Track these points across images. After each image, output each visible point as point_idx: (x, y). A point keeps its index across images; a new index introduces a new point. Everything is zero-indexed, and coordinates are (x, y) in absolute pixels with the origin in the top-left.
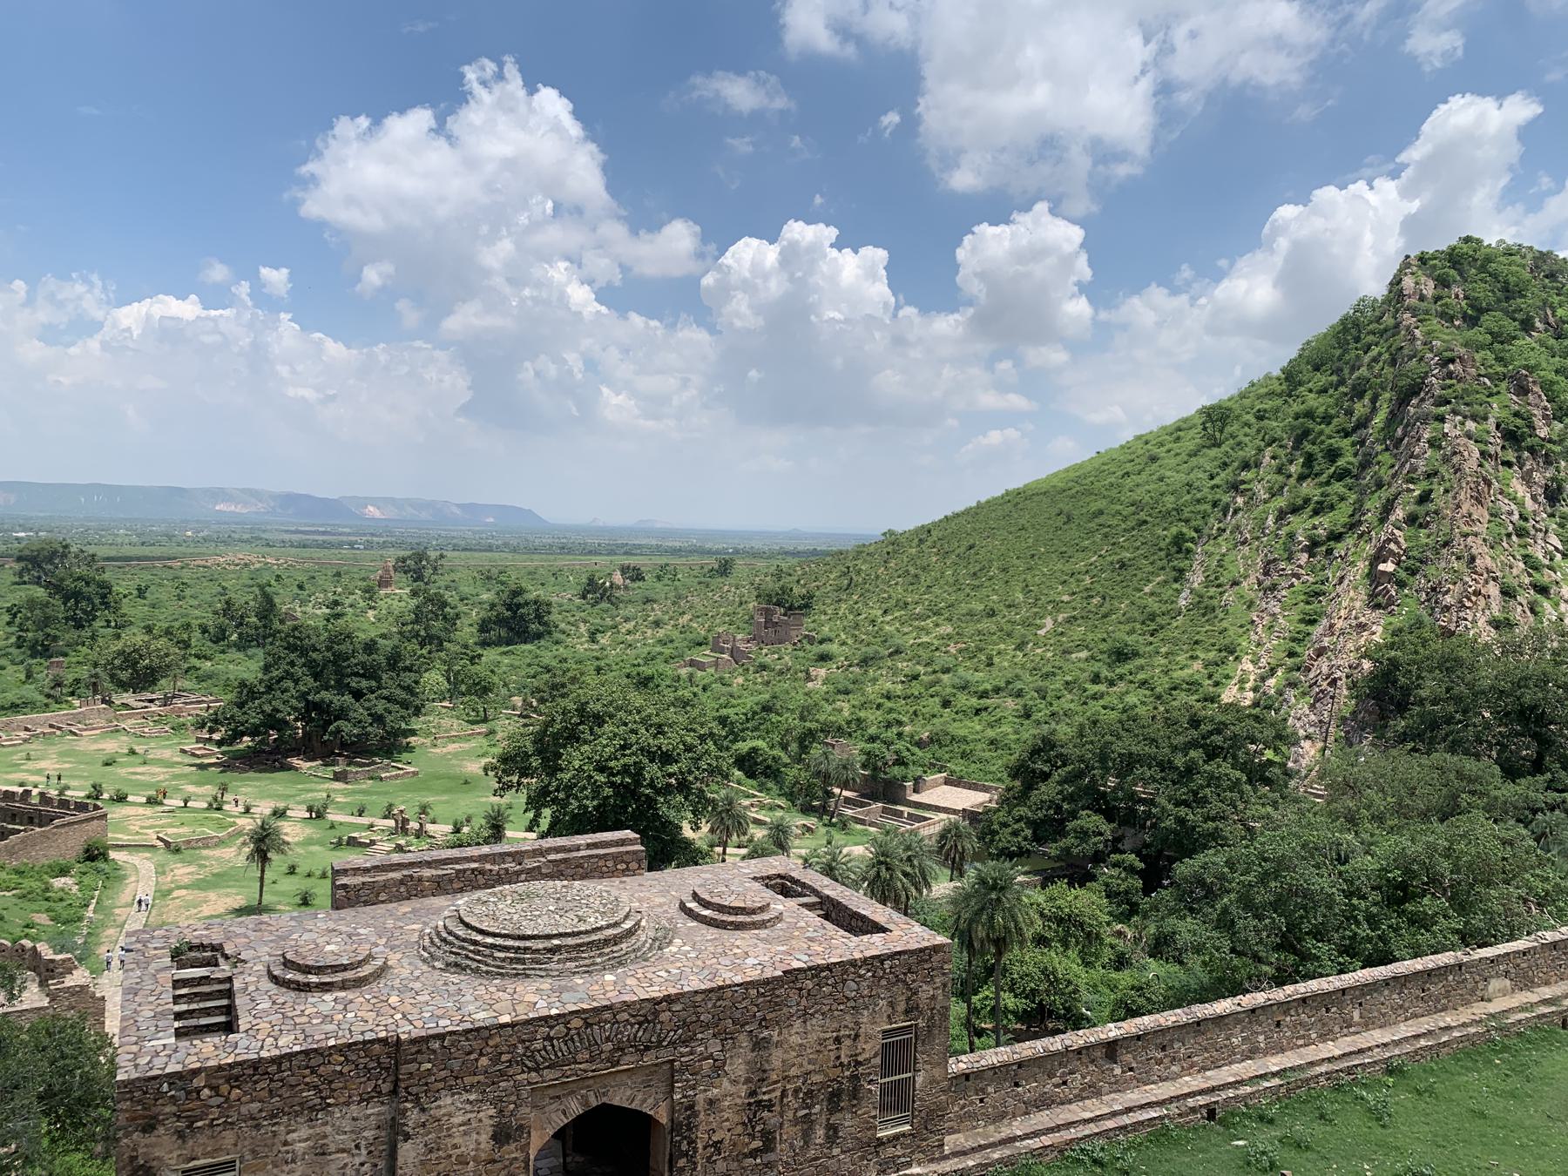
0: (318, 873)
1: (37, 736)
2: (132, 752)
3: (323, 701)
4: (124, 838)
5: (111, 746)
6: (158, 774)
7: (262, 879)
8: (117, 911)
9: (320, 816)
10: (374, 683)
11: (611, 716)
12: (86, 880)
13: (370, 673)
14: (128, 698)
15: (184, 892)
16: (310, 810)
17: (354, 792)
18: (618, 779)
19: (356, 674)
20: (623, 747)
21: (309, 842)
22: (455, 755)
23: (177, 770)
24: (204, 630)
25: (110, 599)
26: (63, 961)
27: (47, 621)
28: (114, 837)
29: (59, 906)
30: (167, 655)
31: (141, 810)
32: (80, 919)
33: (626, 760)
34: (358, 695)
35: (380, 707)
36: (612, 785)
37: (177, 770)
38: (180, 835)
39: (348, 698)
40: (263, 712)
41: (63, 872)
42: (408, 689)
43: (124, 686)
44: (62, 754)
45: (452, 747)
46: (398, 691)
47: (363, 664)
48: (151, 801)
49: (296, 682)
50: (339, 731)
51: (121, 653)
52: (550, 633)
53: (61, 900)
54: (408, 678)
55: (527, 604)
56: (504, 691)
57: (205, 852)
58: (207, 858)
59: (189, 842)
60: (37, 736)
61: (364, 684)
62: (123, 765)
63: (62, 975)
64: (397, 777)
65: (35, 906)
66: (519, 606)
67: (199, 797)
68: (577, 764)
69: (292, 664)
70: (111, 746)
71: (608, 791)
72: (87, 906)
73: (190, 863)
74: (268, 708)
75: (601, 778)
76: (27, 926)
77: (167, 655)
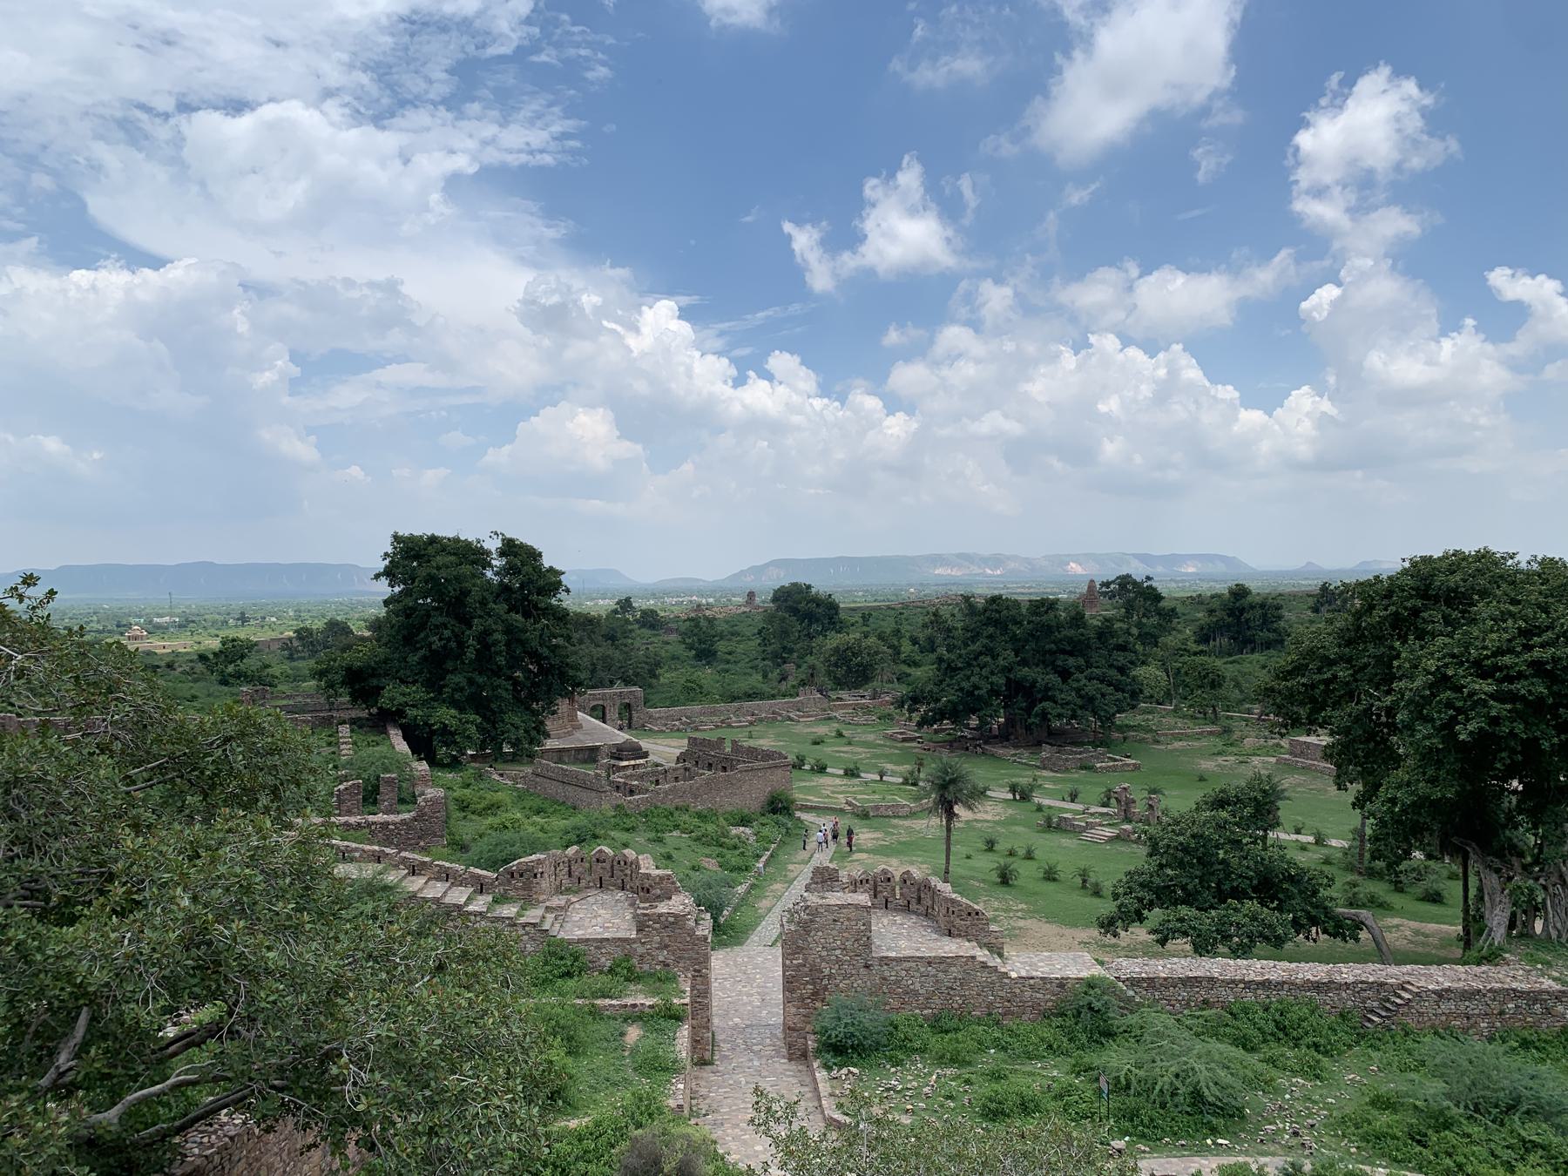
0: (1022, 852)
1: (761, 720)
2: (840, 735)
3: (1024, 678)
4: (814, 800)
5: (822, 730)
6: (861, 753)
7: (948, 838)
8: (790, 867)
9: (1025, 797)
10: (1081, 661)
11: (1484, 594)
12: (766, 831)
13: (1078, 648)
14: (844, 694)
15: (864, 856)
16: (1013, 789)
17: (1063, 780)
18: (1520, 687)
19: (1064, 652)
20: (1525, 633)
21: (1011, 822)
22: (1183, 752)
23: (878, 751)
24: (914, 641)
25: (836, 619)
26: (661, 878)
27: (785, 633)
28: (798, 796)
29: (729, 854)
30: (877, 653)
31: (838, 781)
32: (747, 869)
33: (1537, 653)
34: (1065, 674)
35: (1091, 688)
36: (1512, 697)
37: (878, 751)
38: (869, 801)
39: (1054, 679)
40: (961, 689)
41: (744, 821)
42: (1122, 670)
43: (840, 684)
44: (778, 736)
45: (1178, 744)
46: (1113, 673)
47: (1070, 640)
48: (851, 773)
49: (995, 657)
50: (1044, 715)
51: (836, 650)
52: (1282, 642)
53: (735, 848)
54: (1121, 658)
55: (1252, 607)
56: (1236, 694)
57: (896, 821)
58: (895, 827)
59: (877, 808)
60: (761, 720)
61: (1071, 661)
62: (834, 745)
63: (659, 898)
64: (1114, 769)
65: (707, 851)
66: (1242, 610)
67: (894, 774)
68: (1432, 665)
69: (990, 637)
70: (822, 730)
71: (1496, 708)
72: (759, 856)
73: (876, 829)
74: (965, 685)
75: (1487, 686)
76: (693, 868)
77: (877, 653)
